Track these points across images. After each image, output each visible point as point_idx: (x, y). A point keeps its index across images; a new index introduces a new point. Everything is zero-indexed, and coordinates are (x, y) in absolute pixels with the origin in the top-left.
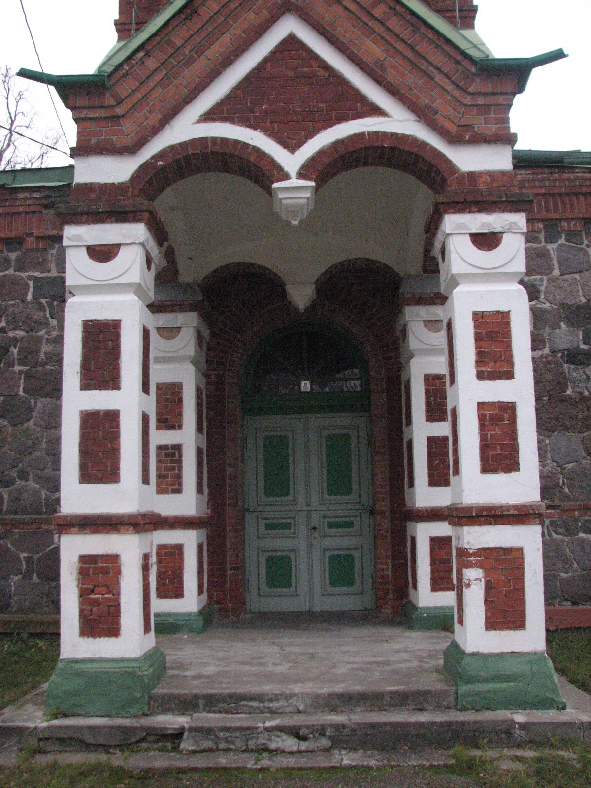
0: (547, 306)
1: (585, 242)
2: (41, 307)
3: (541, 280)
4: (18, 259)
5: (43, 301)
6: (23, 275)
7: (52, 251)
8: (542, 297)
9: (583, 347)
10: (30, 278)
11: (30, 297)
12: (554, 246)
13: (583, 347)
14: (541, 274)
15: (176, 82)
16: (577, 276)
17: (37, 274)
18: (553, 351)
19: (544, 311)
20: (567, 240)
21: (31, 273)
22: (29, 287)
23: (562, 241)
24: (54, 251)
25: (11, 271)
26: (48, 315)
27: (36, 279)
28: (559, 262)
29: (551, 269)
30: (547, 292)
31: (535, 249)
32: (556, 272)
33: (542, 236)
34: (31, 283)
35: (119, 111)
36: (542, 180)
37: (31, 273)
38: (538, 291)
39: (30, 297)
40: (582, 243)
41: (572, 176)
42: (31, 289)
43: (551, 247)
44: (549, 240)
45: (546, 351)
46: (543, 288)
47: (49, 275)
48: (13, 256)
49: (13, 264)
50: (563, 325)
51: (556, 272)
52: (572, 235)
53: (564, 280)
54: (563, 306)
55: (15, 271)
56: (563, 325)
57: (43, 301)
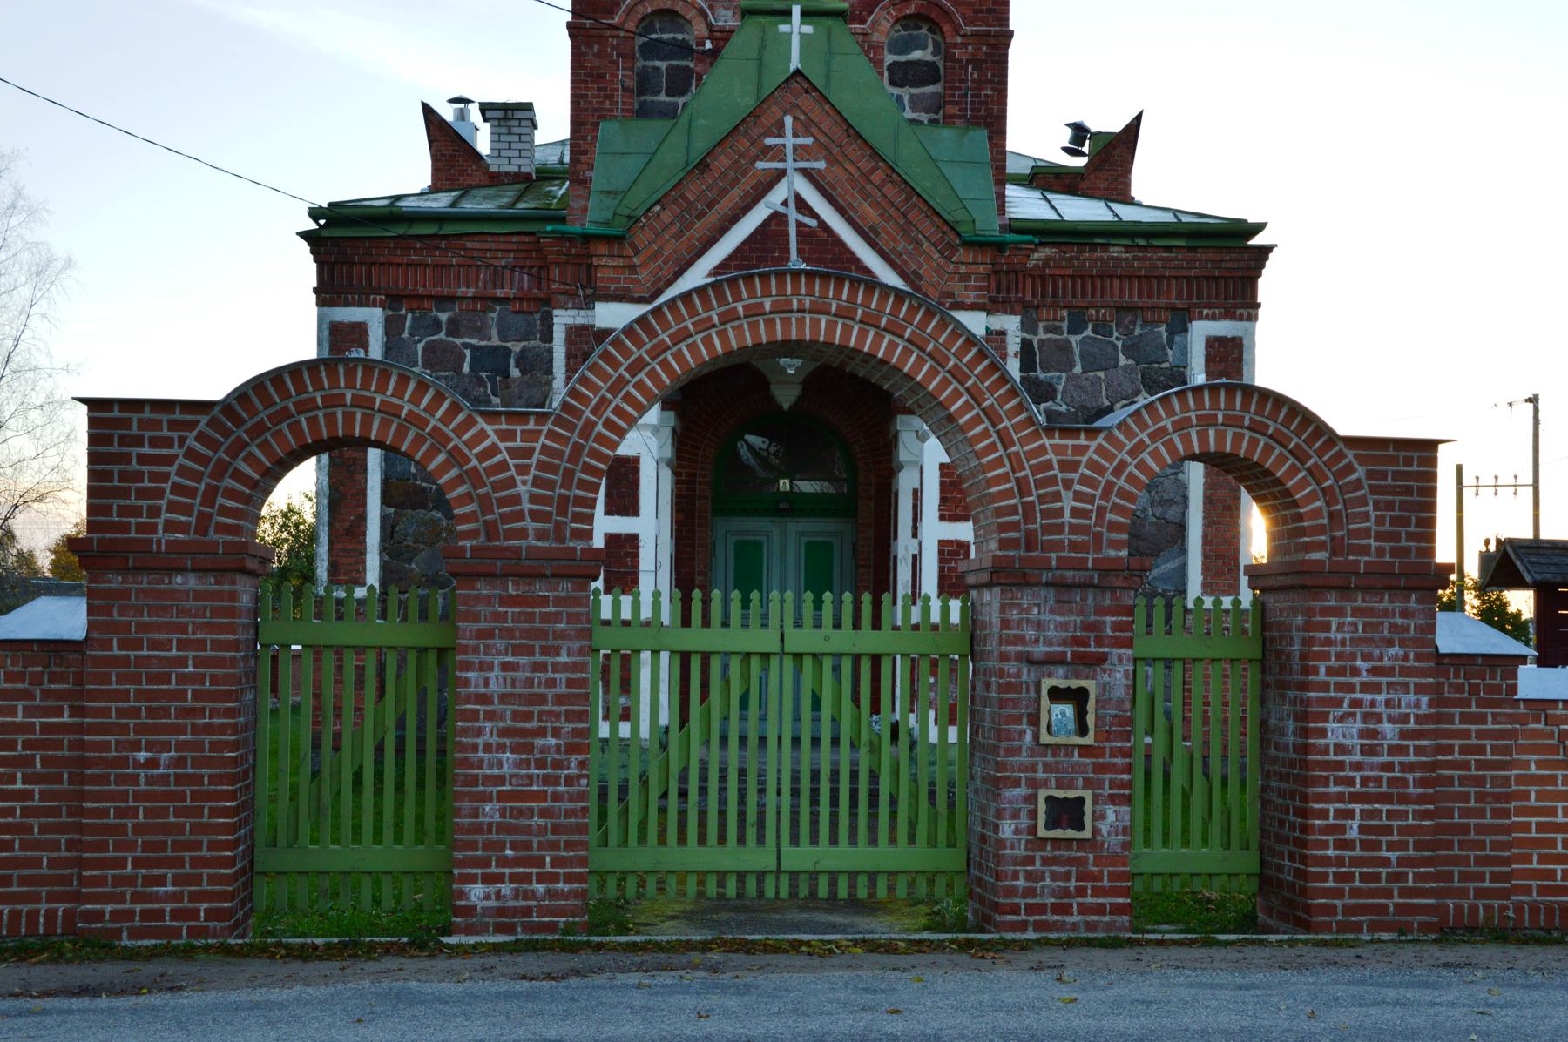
0: (1064, 408)
1: (1116, 334)
2: (480, 381)
3: (1060, 378)
4: (451, 321)
5: (484, 374)
6: (458, 341)
7: (492, 315)
8: (1059, 397)
10: (466, 346)
11: (466, 369)
12: (1078, 338)
14: (1061, 371)
15: (688, 234)
16: (1101, 374)
17: (474, 342)
19: (1059, 413)
20: (1094, 331)
21: (467, 340)
22: (465, 356)
23: (1088, 332)
24: (494, 315)
25: (442, 335)
26: (489, 392)
27: (473, 348)
28: (1082, 356)
29: (1072, 365)
30: (1064, 392)
31: (1056, 341)
32: (1078, 369)
33: (1065, 325)
34: (468, 352)
35: (636, 260)
36: (1071, 259)
37: (467, 340)
38: (1055, 390)
39: (466, 369)
40: (1111, 336)
41: (1105, 256)
42: (468, 359)
43: (1075, 339)
44: (1072, 331)
46: (1060, 388)
47: (489, 344)
48: (444, 317)
49: (444, 327)
51: (1078, 369)
52: (1101, 328)
53: (1087, 379)
54: (1083, 408)
55: (447, 335)
57: (484, 374)
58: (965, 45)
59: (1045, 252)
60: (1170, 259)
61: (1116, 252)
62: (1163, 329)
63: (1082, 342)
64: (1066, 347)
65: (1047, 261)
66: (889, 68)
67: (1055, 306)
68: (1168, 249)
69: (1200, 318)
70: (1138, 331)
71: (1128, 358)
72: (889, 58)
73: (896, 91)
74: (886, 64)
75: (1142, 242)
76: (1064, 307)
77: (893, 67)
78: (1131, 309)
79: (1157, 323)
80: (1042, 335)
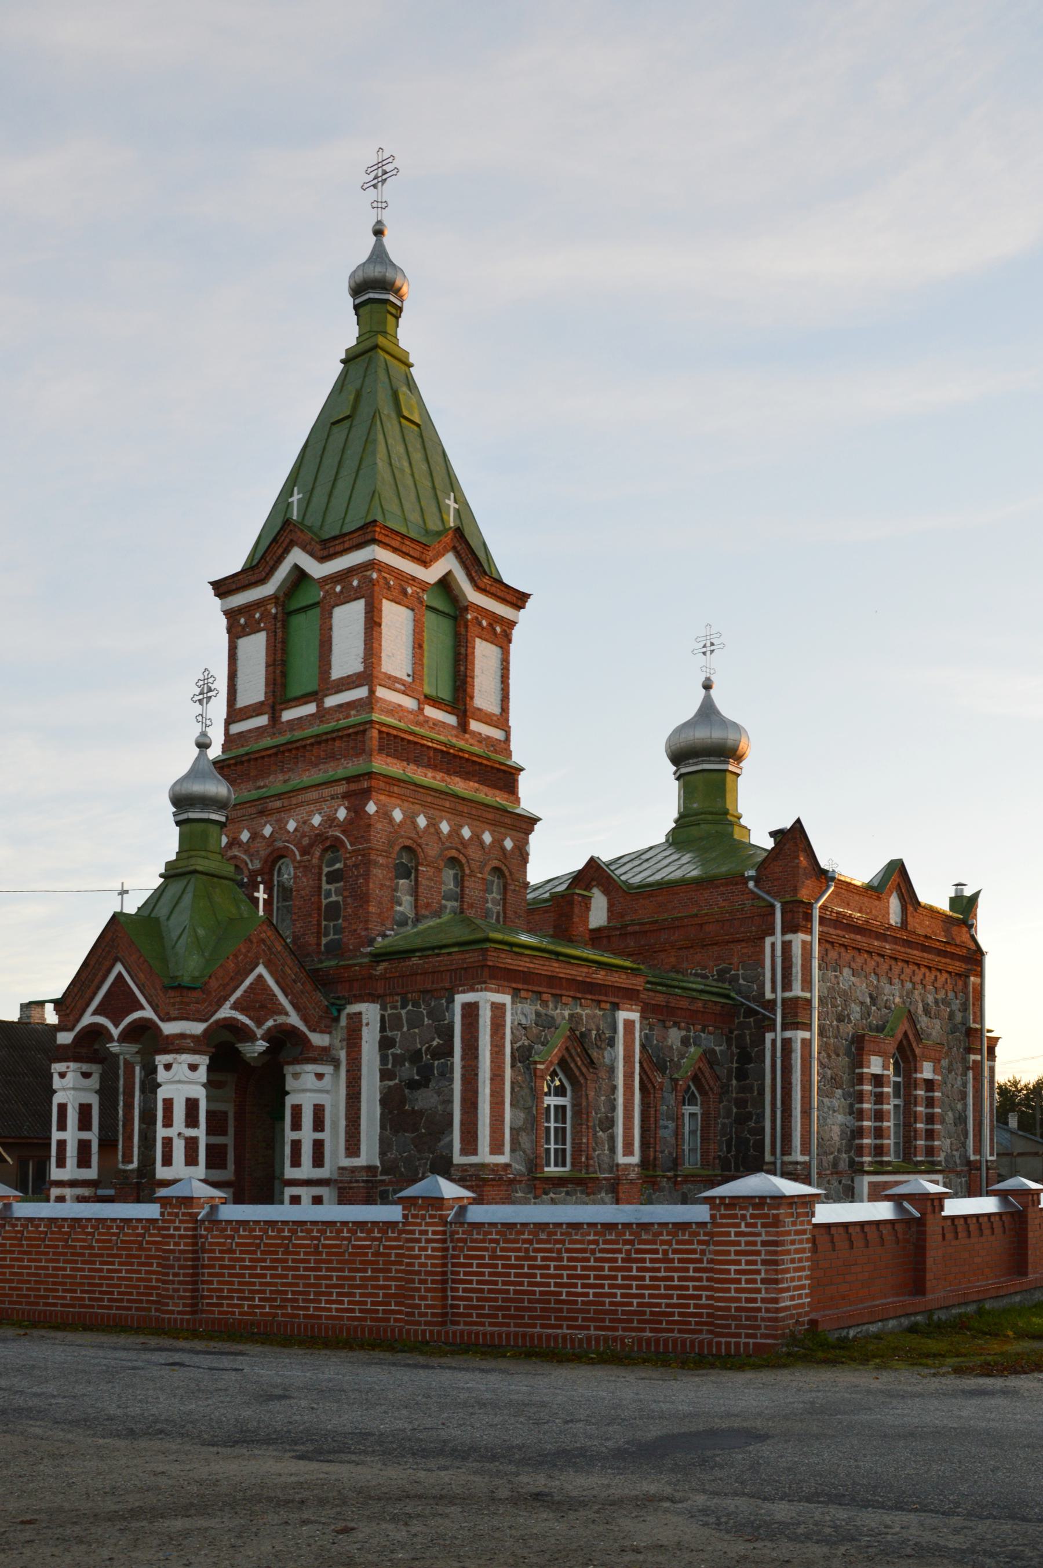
0: (399, 1051)
9: (417, 1078)
13: (417, 1078)
16: (416, 1030)
18: (401, 1081)
19: (397, 1055)
23: (410, 1007)
32: (405, 1029)
33: (399, 1004)
43: (403, 1012)
44: (403, 1007)
45: (397, 1081)
50: (407, 1064)
51: (405, 1029)
52: (416, 1004)
56: (407, 1064)
58: (351, 857)
59: (381, 967)
60: (440, 961)
61: (415, 960)
62: (443, 1001)
63: (407, 1013)
64: (399, 1017)
65: (386, 969)
66: (326, 875)
67: (391, 995)
68: (449, 954)
69: (458, 993)
70: (433, 1004)
71: (429, 1019)
72: (326, 870)
73: (329, 887)
74: (324, 873)
75: (437, 951)
76: (397, 994)
77: (328, 874)
78: (428, 992)
79: (441, 998)
80: (389, 1012)
